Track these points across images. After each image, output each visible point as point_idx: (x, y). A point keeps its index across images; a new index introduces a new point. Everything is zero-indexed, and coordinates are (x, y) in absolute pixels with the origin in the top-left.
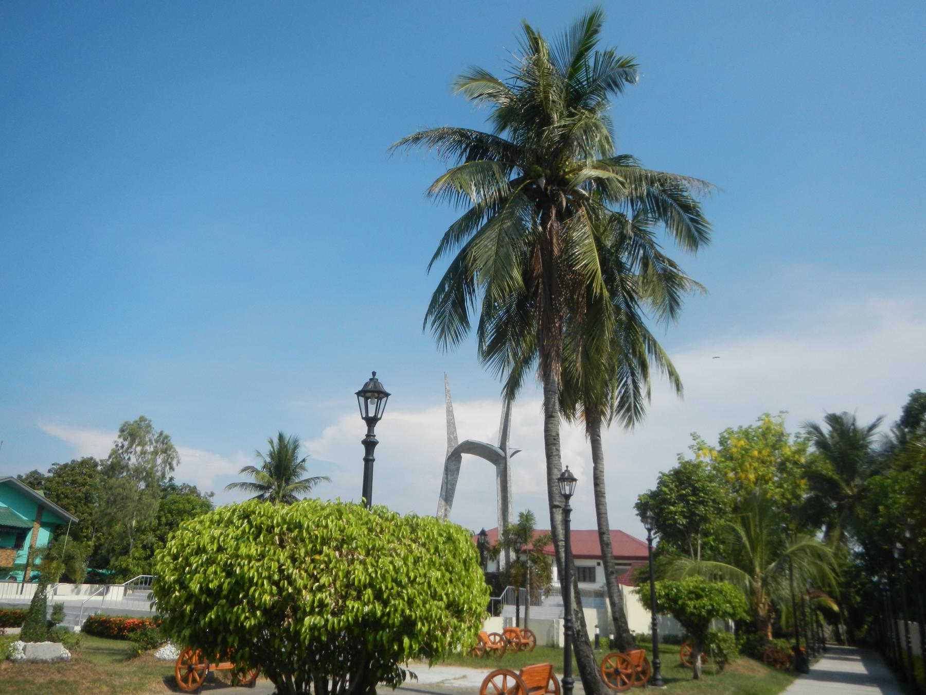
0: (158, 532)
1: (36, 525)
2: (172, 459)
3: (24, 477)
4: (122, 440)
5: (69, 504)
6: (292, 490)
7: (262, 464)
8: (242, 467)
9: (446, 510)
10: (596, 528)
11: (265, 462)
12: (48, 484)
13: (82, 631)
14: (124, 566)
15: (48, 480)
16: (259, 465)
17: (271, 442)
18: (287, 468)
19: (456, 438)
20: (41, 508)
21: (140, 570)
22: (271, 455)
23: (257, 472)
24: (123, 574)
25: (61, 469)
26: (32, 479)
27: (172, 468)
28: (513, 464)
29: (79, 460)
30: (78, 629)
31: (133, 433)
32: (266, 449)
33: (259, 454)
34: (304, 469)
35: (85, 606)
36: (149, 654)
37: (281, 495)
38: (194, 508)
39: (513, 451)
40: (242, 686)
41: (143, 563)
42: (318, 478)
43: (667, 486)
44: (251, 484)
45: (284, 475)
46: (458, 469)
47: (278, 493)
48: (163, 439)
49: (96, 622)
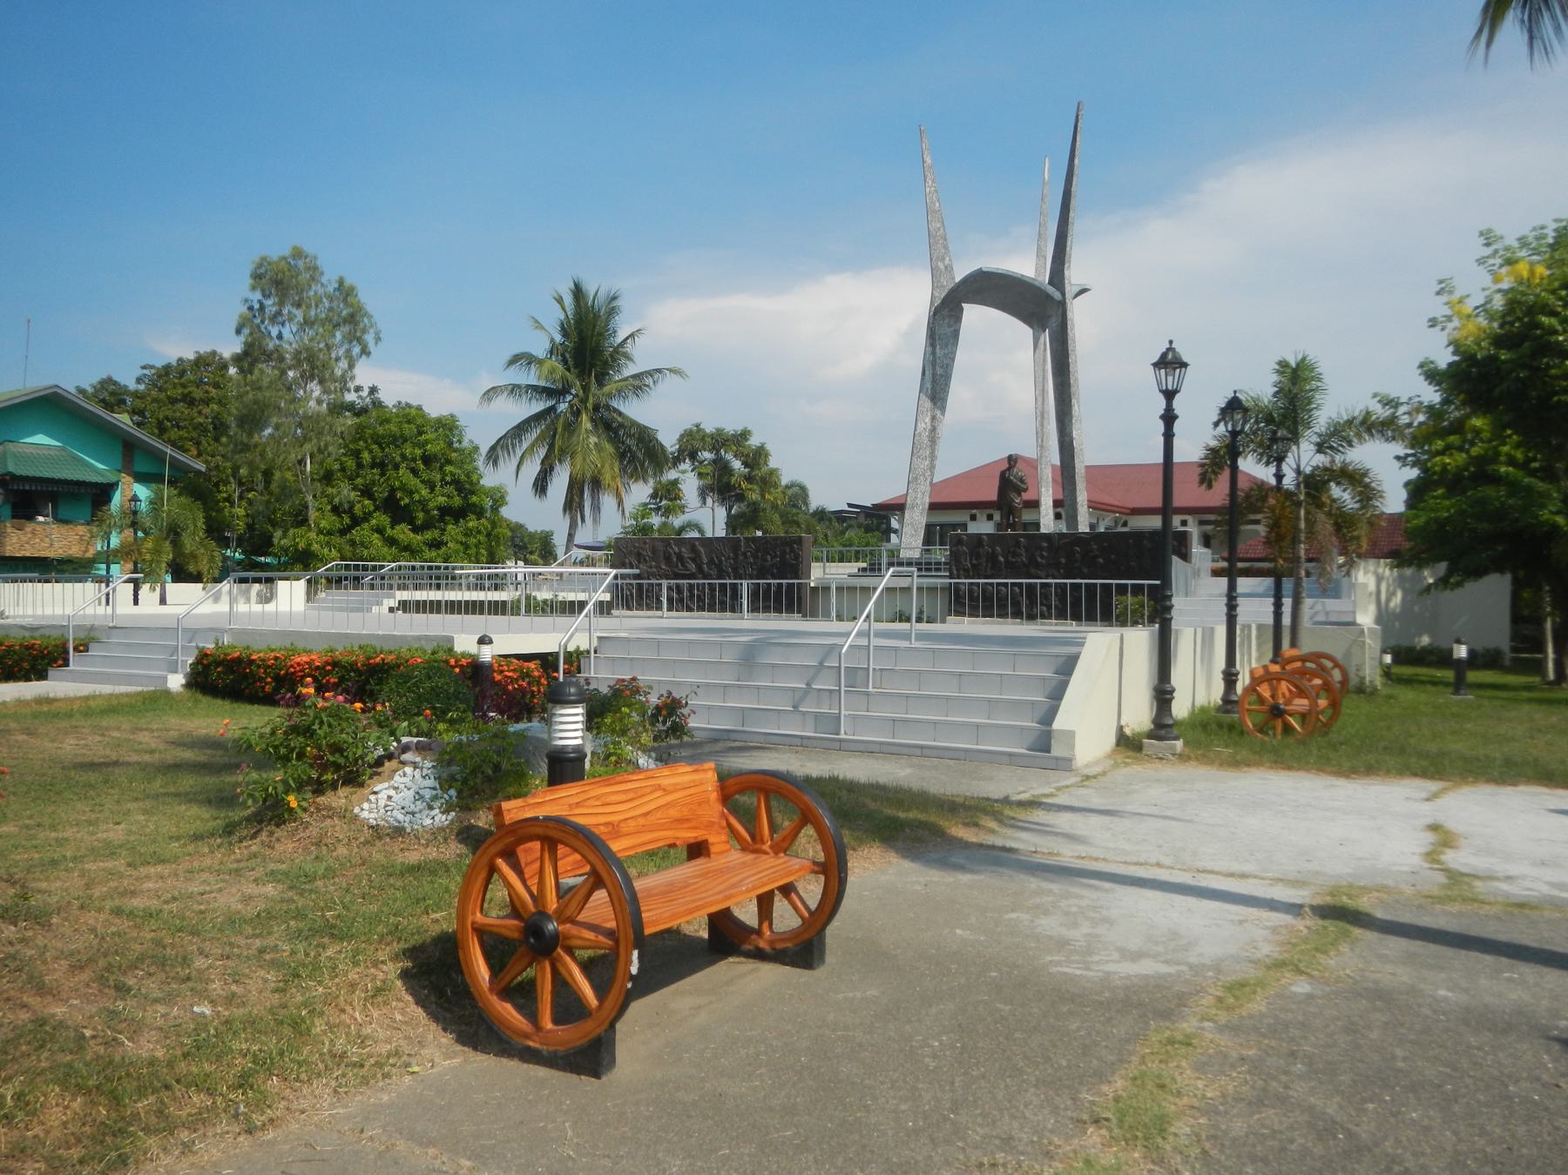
0: (359, 481)
1: (126, 479)
2: (364, 331)
3: (90, 390)
4: (257, 296)
5: (181, 438)
6: (610, 396)
7: (547, 346)
8: (507, 356)
9: (933, 418)
10: (1161, 460)
11: (552, 340)
12: (139, 404)
13: (188, 685)
14: (302, 546)
15: (136, 395)
16: (540, 348)
17: (560, 300)
18: (597, 351)
19: (949, 269)
20: (129, 450)
21: (334, 553)
22: (565, 332)
23: (540, 362)
24: (302, 561)
25: (160, 376)
26: (105, 395)
27: (365, 352)
28: (1081, 316)
29: (191, 356)
30: (176, 682)
31: (280, 281)
32: (553, 318)
33: (538, 325)
34: (628, 357)
35: (187, 624)
36: (332, 813)
37: (590, 406)
38: (420, 433)
39: (1077, 289)
40: (760, 955)
41: (337, 540)
42: (659, 371)
43: (1554, 314)
44: (529, 386)
45: (592, 366)
46: (956, 335)
47: (584, 401)
48: (345, 292)
49: (218, 664)
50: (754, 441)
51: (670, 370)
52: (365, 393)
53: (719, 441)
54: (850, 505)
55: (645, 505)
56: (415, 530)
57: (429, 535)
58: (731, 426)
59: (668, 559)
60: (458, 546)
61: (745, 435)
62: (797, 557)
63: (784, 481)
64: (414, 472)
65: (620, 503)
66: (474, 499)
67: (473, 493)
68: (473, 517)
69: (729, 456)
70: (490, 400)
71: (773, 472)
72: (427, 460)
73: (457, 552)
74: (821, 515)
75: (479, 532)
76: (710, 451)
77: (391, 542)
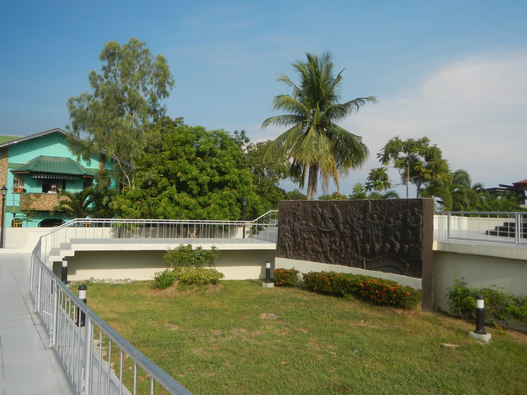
16: (289, 92)
18: (319, 91)
27: (166, 94)
33: (286, 80)
42: (358, 99)
50: (431, 145)
51: (368, 99)
52: (239, 134)
53: (409, 146)
54: (501, 185)
55: (368, 184)
56: (193, 196)
57: (201, 199)
58: (416, 138)
59: (315, 218)
60: (217, 207)
61: (425, 140)
62: (418, 221)
63: (453, 168)
64: (190, 161)
65: (336, 179)
66: (227, 177)
67: (227, 173)
68: (226, 188)
69: (417, 155)
70: (266, 125)
71: (443, 162)
72: (200, 154)
73: (215, 209)
74: (479, 189)
75: (230, 197)
76: (405, 151)
77: (177, 204)
